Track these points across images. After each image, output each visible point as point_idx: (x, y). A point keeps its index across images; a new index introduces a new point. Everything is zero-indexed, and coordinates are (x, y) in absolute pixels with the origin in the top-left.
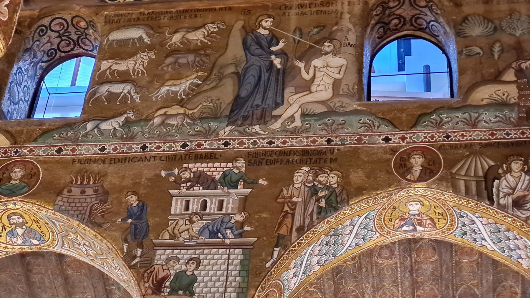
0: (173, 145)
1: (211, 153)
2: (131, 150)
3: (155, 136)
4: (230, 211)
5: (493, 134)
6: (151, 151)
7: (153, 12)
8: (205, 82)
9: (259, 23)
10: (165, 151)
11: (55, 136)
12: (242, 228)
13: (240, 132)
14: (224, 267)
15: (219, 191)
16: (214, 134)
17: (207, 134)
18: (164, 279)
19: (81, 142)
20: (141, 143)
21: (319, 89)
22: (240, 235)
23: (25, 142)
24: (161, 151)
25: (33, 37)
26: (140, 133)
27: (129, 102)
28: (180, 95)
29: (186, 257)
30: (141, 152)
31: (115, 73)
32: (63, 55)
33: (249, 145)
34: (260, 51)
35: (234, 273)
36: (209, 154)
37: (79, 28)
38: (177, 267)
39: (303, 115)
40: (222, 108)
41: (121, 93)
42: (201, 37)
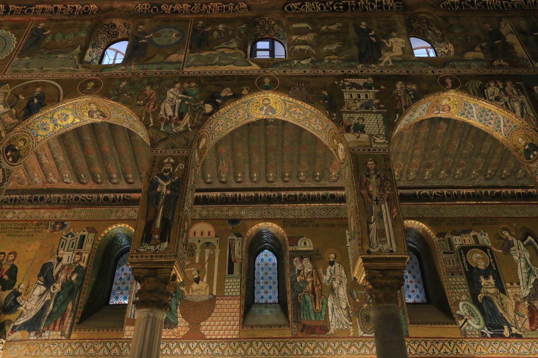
4: (371, 99)
5: (478, 71)
12: (379, 106)
14: (375, 121)
15: (364, 90)
17: (352, 67)
18: (350, 126)
21: (396, 51)
22: (380, 108)
23: (267, 68)
29: (357, 117)
32: (260, 37)
33: (372, 72)
35: (381, 124)
38: (354, 121)
39: (393, 61)
42: (335, 28)
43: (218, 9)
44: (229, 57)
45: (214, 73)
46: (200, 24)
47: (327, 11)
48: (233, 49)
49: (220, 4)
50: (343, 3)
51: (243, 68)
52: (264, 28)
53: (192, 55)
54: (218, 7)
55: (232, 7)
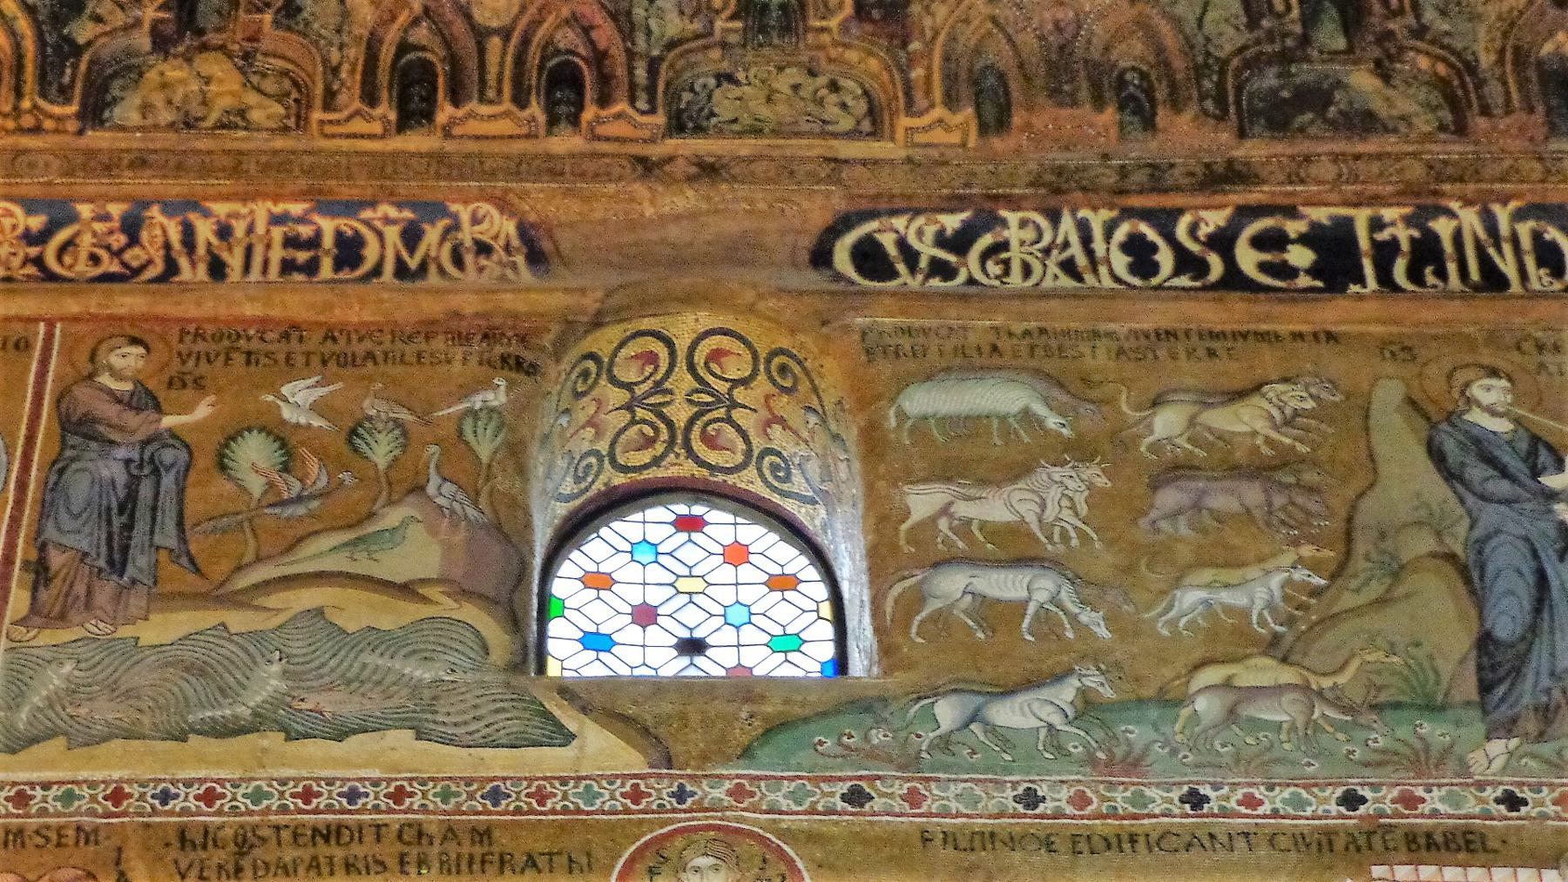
0: (1305, 794)
1: (1468, 832)
2: (1145, 806)
3: (1224, 760)
6: (1225, 813)
7: (1042, 331)
8: (1340, 581)
9: (1463, 393)
10: (1283, 817)
11: (821, 743)
13: (1547, 762)
16: (1451, 765)
17: (1422, 761)
19: (933, 769)
20: (1180, 784)
23: (704, 758)
24: (1265, 816)
25: (560, 394)
26: (1156, 747)
27: (1070, 635)
28: (1262, 622)
30: (1188, 816)
31: (975, 528)
34: (1503, 487)
36: (1459, 834)
37: (710, 379)
40: (1445, 679)
41: (1023, 604)
42: (1261, 426)
43: (277, 254)
44: (371, 659)
45: (243, 803)
46: (117, 375)
47: (1184, 281)
48: (407, 590)
49: (296, 208)
50: (1315, 226)
51: (498, 762)
52: (657, 410)
53: (48, 637)
54: (278, 233)
55: (393, 234)
